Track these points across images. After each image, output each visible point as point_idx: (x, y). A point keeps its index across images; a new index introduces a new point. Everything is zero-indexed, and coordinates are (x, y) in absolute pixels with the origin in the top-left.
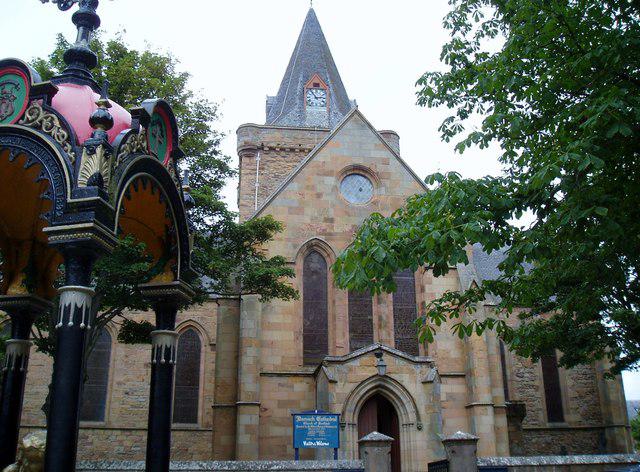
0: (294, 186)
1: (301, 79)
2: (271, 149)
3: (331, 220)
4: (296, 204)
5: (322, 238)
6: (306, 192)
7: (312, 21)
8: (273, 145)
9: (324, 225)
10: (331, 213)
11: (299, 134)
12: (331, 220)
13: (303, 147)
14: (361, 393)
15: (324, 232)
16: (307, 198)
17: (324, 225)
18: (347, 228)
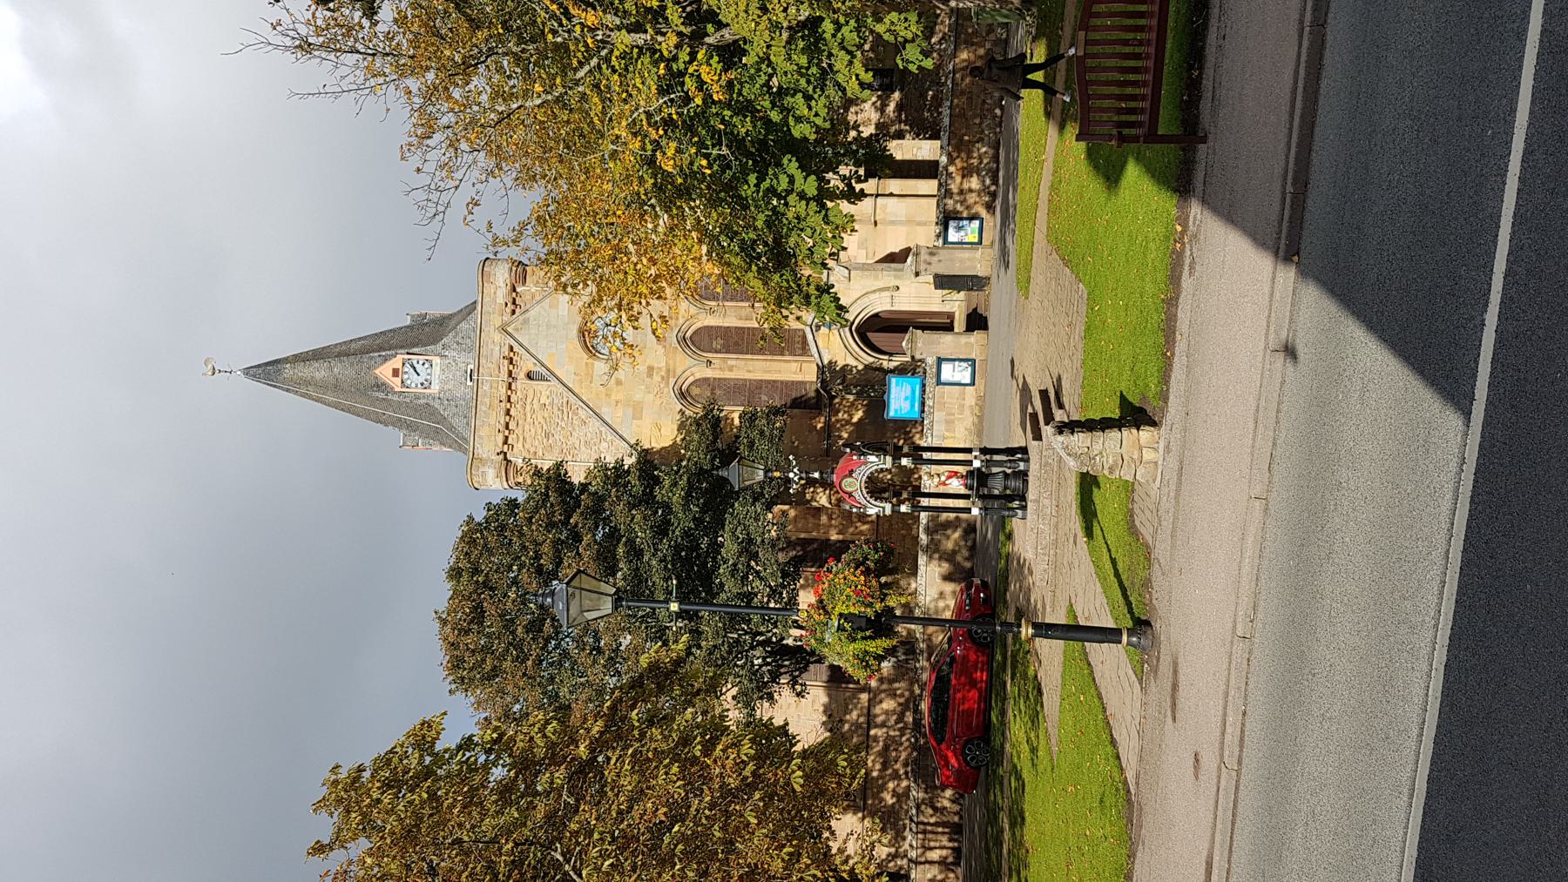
0: (606, 412)
1: (382, 395)
2: (505, 442)
3: (651, 369)
4: (630, 411)
5: (672, 381)
6: (613, 397)
7: (267, 372)
8: (500, 438)
9: (657, 378)
10: (642, 368)
11: (484, 401)
12: (651, 369)
13: (504, 398)
14: (857, 349)
15: (665, 379)
16: (620, 396)
17: (657, 378)
18: (661, 350)
